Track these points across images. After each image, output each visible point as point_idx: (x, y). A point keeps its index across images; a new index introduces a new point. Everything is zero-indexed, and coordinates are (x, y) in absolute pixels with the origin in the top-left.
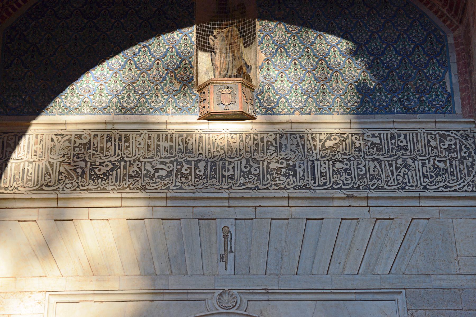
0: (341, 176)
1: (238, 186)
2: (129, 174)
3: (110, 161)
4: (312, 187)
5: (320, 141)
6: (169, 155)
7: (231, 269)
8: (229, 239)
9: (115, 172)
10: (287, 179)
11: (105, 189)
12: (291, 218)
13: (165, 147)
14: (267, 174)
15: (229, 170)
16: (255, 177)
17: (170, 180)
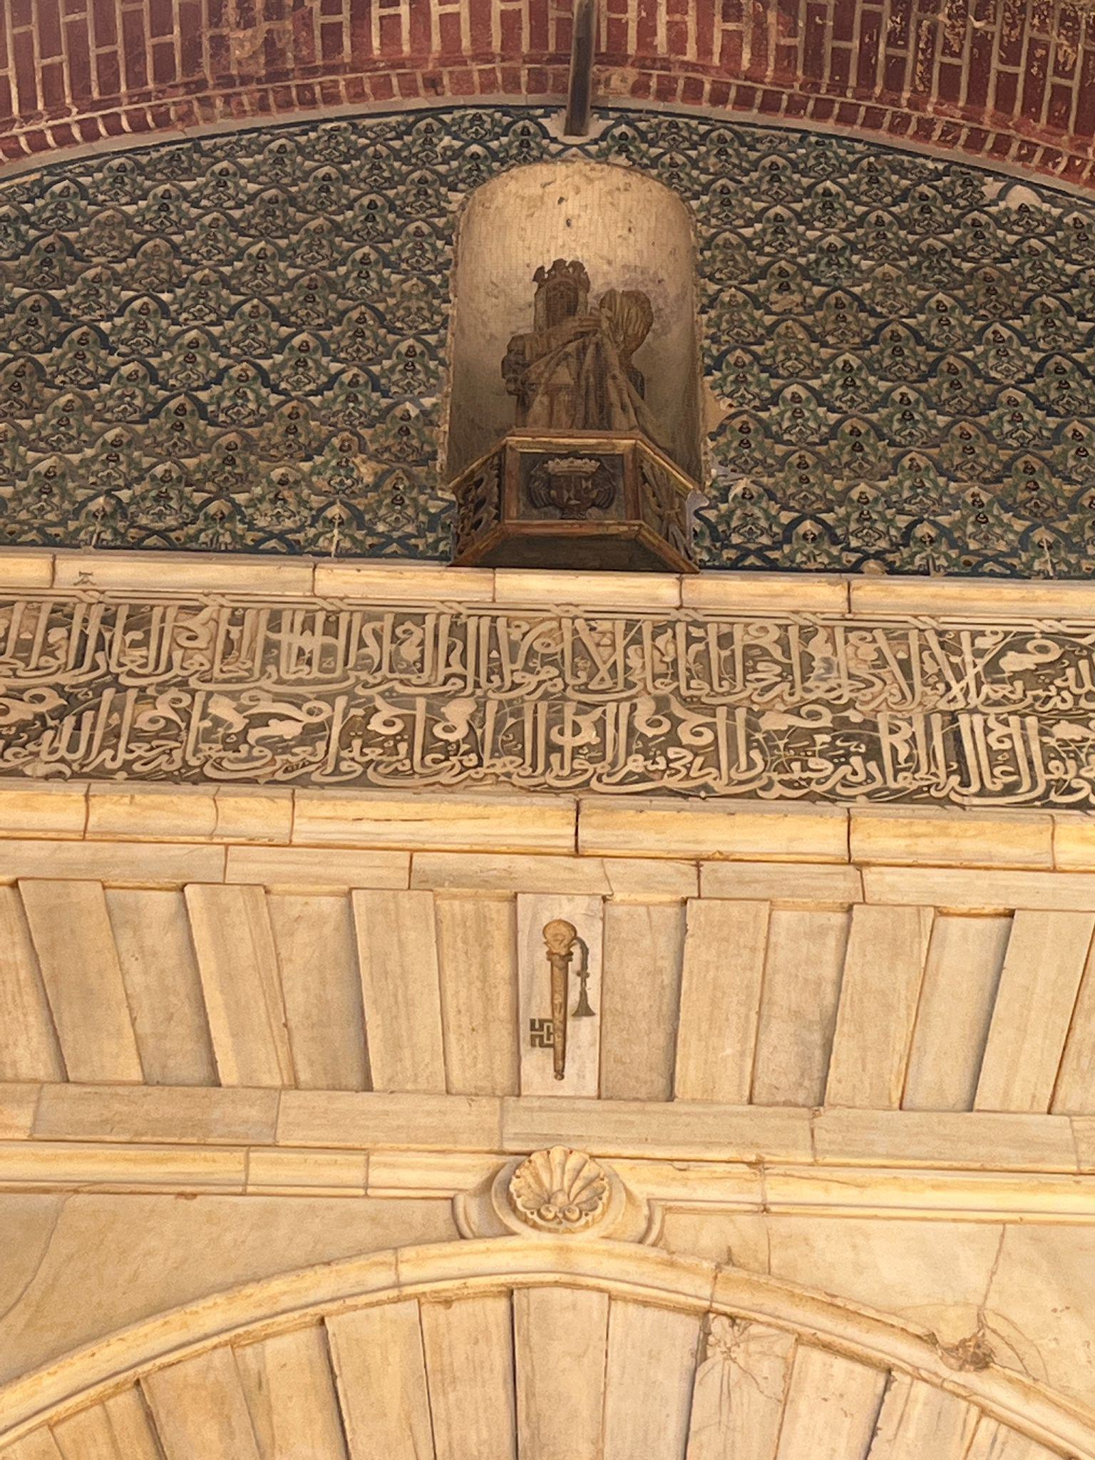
0: (1080, 767)
1: (620, 783)
2: (132, 729)
3: (58, 688)
4: (954, 797)
5: (979, 653)
6: (316, 674)
7: (581, 1076)
8: (575, 965)
9: (70, 721)
10: (837, 766)
11: (16, 773)
12: (864, 903)
13: (301, 652)
14: (749, 749)
15: (577, 730)
16: (696, 755)
17: (313, 754)
